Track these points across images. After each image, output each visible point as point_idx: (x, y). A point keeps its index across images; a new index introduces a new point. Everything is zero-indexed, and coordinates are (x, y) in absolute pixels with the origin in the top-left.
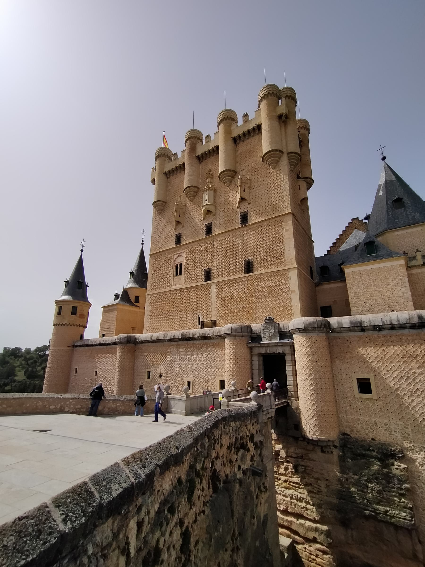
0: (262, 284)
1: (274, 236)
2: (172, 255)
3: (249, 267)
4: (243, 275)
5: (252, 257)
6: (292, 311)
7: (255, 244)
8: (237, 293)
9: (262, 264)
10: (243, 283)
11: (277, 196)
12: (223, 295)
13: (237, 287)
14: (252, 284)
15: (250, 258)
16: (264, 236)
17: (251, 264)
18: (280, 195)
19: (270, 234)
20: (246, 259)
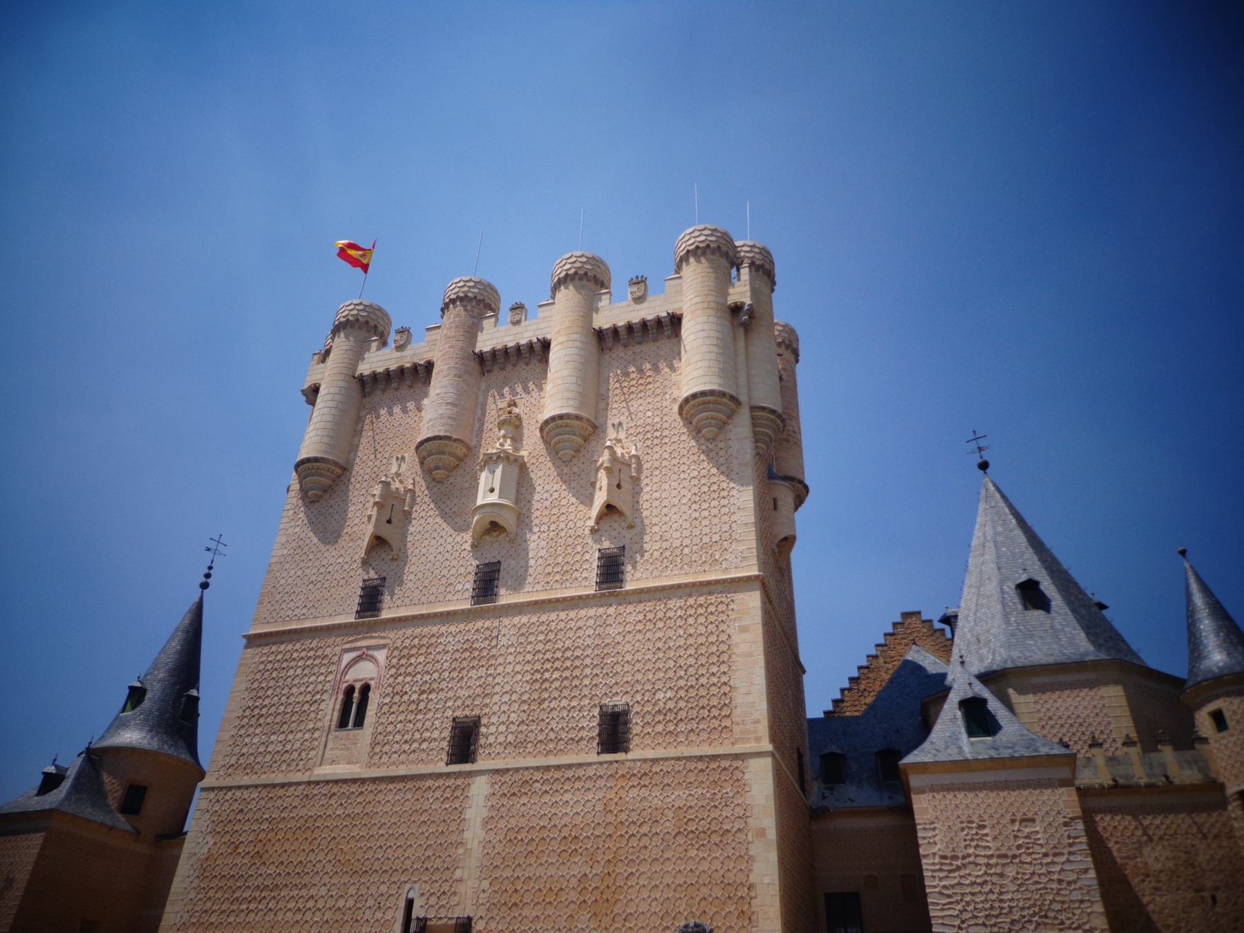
0: (655, 797)
1: (702, 640)
2: (338, 649)
3: (614, 731)
4: (593, 757)
5: (626, 699)
6: (753, 902)
7: (639, 656)
8: (566, 820)
9: (660, 728)
10: (589, 784)
11: (716, 520)
12: (513, 822)
13: (567, 797)
14: (622, 793)
15: (620, 701)
16: (670, 633)
17: (621, 719)
18: (726, 518)
19: (692, 631)
20: (606, 701)
